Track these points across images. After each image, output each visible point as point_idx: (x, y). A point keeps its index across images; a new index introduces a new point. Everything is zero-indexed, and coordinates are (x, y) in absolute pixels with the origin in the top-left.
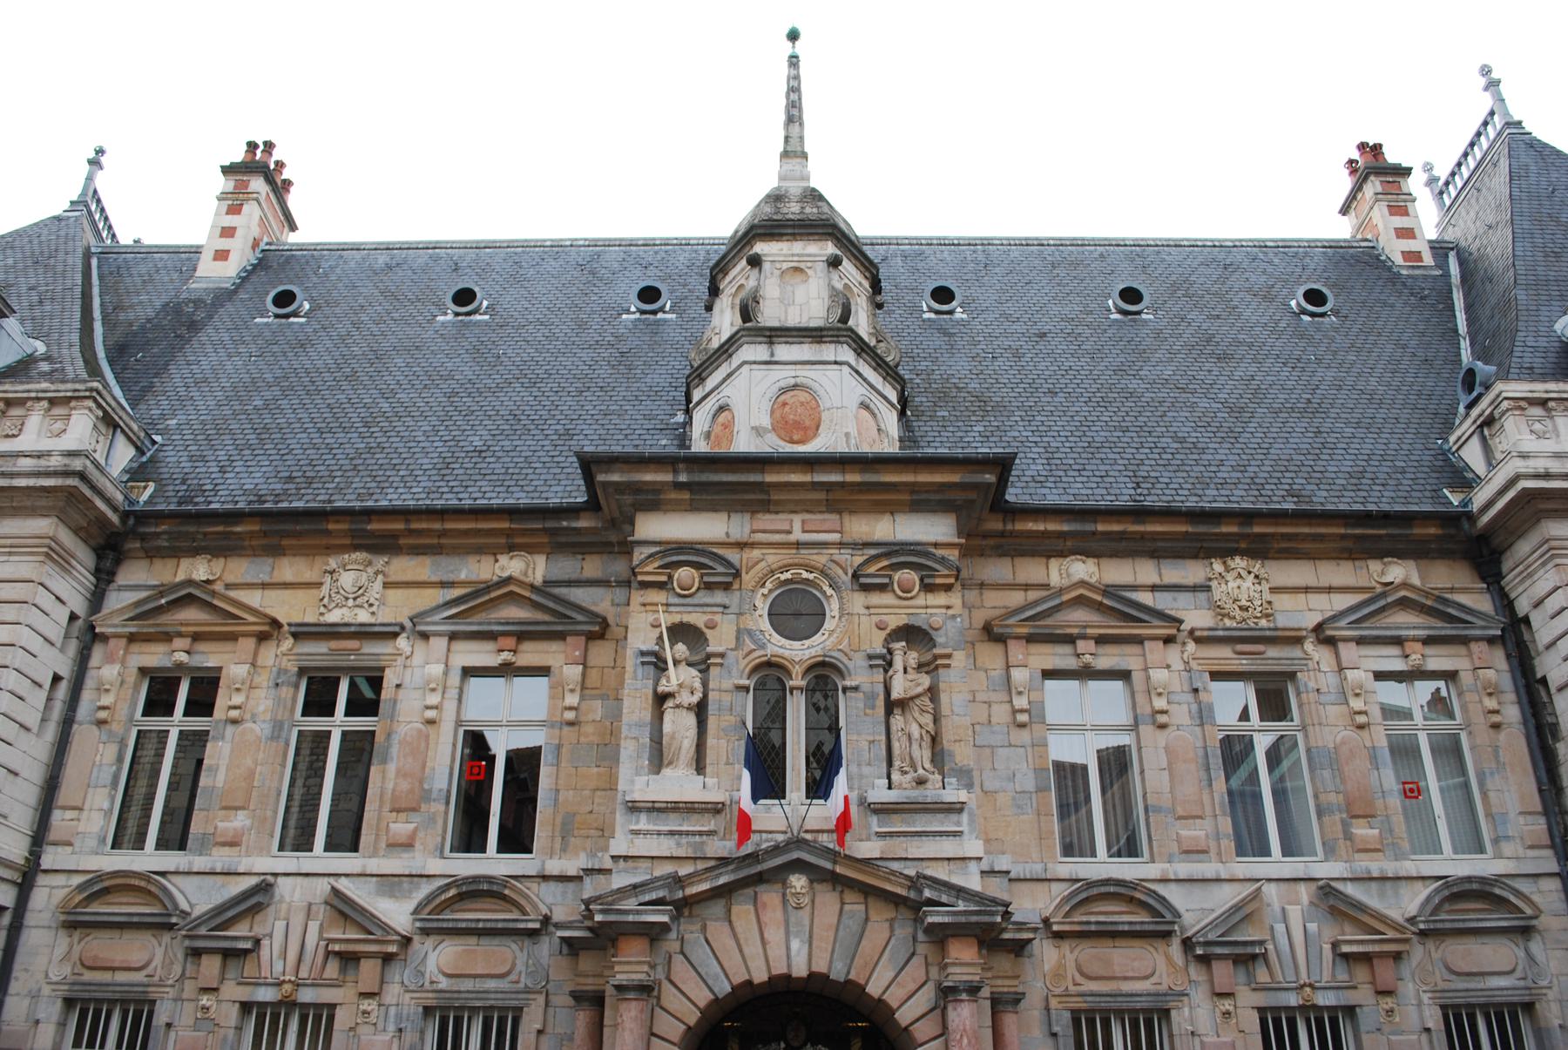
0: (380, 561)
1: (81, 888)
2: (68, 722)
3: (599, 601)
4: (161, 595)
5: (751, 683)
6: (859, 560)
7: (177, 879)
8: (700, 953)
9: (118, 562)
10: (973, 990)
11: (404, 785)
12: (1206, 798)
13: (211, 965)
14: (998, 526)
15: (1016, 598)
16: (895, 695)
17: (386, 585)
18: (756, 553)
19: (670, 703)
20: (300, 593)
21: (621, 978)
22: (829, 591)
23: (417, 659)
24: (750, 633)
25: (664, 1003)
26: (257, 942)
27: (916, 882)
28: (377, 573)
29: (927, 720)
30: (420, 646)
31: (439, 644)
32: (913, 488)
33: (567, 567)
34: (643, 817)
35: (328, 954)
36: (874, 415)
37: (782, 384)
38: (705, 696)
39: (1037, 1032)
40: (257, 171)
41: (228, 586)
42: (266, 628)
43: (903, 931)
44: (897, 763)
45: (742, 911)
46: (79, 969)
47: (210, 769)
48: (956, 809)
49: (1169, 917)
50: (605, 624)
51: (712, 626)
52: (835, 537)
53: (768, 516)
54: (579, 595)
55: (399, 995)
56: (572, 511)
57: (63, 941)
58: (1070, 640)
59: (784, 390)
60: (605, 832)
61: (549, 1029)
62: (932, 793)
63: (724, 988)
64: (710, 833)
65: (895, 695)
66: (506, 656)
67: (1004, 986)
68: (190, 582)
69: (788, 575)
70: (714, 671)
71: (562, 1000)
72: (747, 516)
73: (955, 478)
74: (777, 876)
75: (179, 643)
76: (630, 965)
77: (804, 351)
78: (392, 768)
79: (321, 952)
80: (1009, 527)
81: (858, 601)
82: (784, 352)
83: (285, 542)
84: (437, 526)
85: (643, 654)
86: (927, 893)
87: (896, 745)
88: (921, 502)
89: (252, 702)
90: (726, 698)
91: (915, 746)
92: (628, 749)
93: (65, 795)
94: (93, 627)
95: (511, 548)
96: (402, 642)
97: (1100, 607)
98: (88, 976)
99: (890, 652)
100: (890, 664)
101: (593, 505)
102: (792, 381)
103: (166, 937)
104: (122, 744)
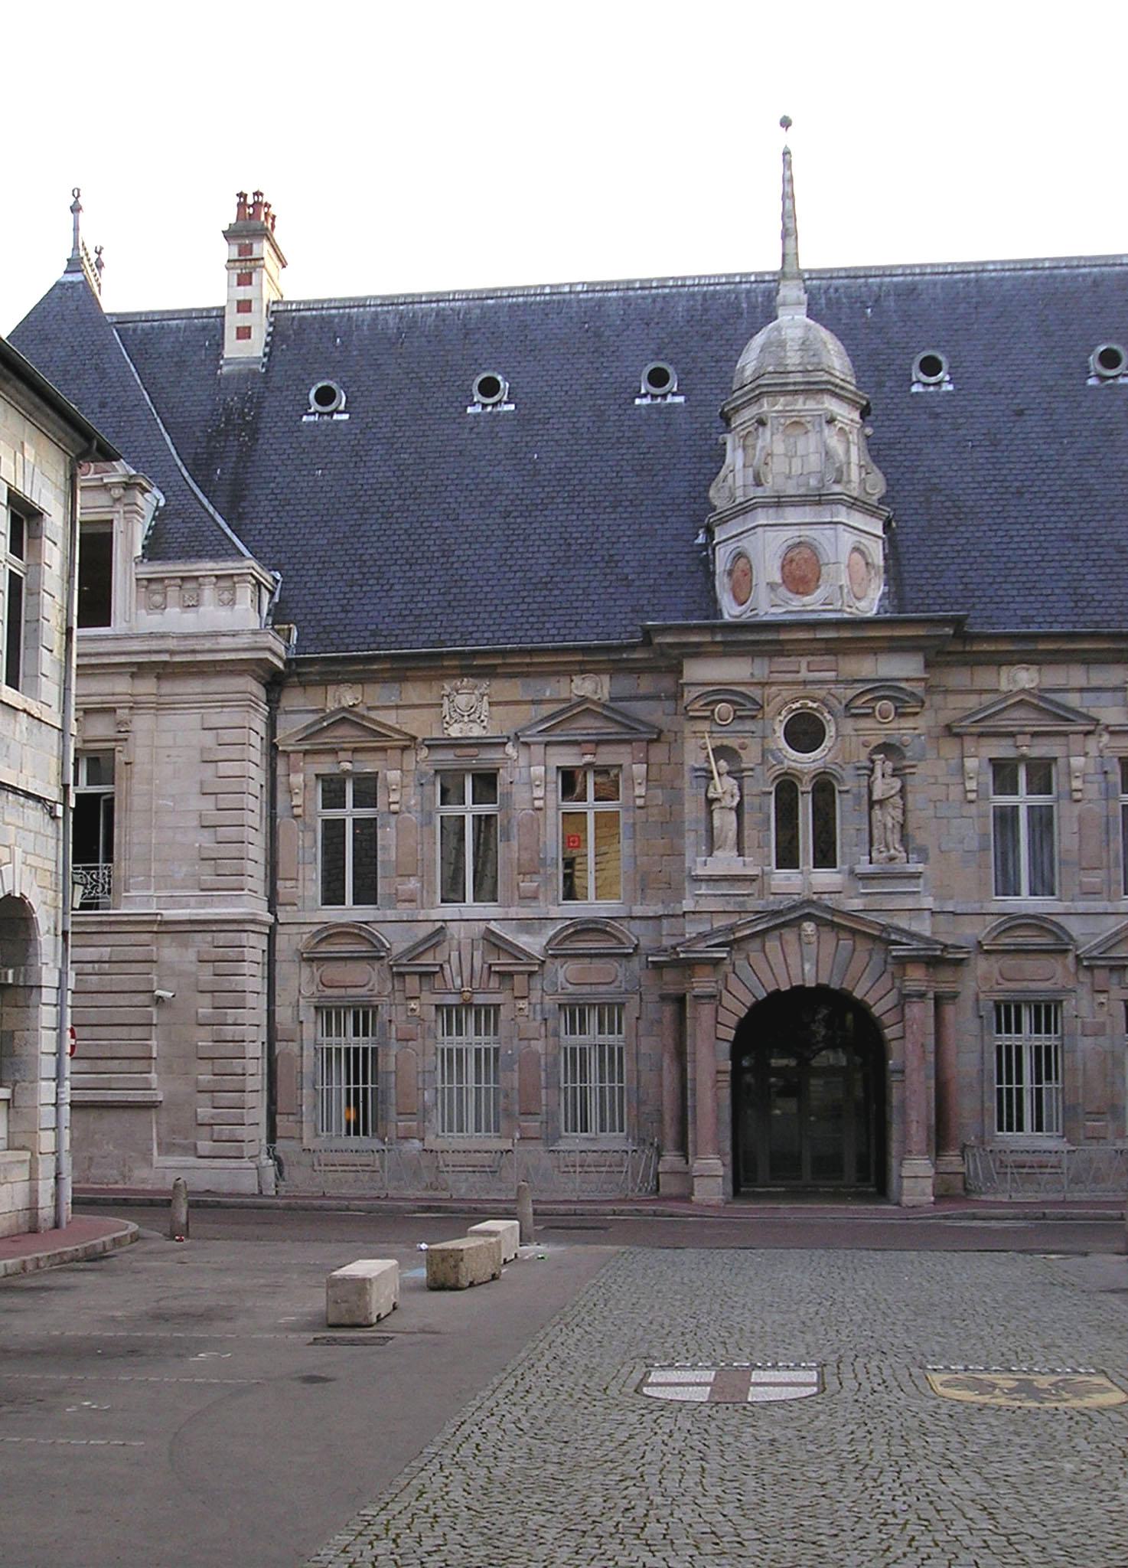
0: (484, 685)
1: (314, 935)
2: (272, 818)
3: (655, 713)
4: (323, 719)
5: (772, 789)
6: (850, 693)
7: (374, 925)
8: (745, 972)
9: (281, 690)
10: (922, 995)
11: (526, 856)
12: (1104, 855)
13: (413, 983)
14: (960, 648)
15: (972, 701)
16: (875, 797)
17: (490, 704)
18: (774, 689)
19: (716, 805)
20: (425, 711)
21: (697, 991)
22: (829, 717)
23: (522, 762)
24: (772, 752)
25: (724, 1003)
26: (441, 966)
27: (884, 928)
28: (483, 695)
29: (898, 813)
30: (523, 750)
31: (538, 751)
32: (891, 638)
33: (627, 684)
34: (704, 885)
35: (490, 971)
36: (862, 553)
37: (790, 542)
38: (741, 797)
39: (969, 1013)
40: (251, 226)
41: (369, 709)
42: (407, 743)
43: (878, 957)
44: (875, 847)
45: (772, 944)
46: (321, 987)
47: (383, 847)
48: (916, 876)
49: (1066, 939)
50: (661, 732)
51: (743, 747)
52: (831, 675)
53: (782, 659)
54: (639, 709)
55: (542, 997)
56: (632, 647)
57: (306, 971)
58: (1012, 735)
59: (791, 548)
60: (673, 889)
61: (644, 1016)
62: (898, 867)
63: (762, 995)
64: (748, 895)
65: (875, 797)
66: (588, 758)
67: (944, 988)
68: (343, 709)
69: (798, 705)
70: (747, 782)
71: (652, 997)
72: (766, 660)
73: (922, 632)
74: (795, 923)
75: (342, 755)
76: (702, 983)
77: (806, 514)
78: (514, 843)
79: (485, 971)
80: (968, 648)
81: (849, 726)
82: (792, 515)
83: (408, 674)
84: (528, 660)
85: (697, 770)
86: (893, 937)
87: (875, 832)
88: (896, 647)
89: (405, 798)
90: (757, 801)
91: (889, 833)
92: (690, 838)
93: (281, 872)
94: (274, 747)
95: (582, 672)
96: (510, 749)
97: (1036, 707)
98: (329, 992)
99: (873, 761)
100: (872, 770)
101: (647, 642)
102: (798, 540)
103: (377, 965)
104: (315, 831)
